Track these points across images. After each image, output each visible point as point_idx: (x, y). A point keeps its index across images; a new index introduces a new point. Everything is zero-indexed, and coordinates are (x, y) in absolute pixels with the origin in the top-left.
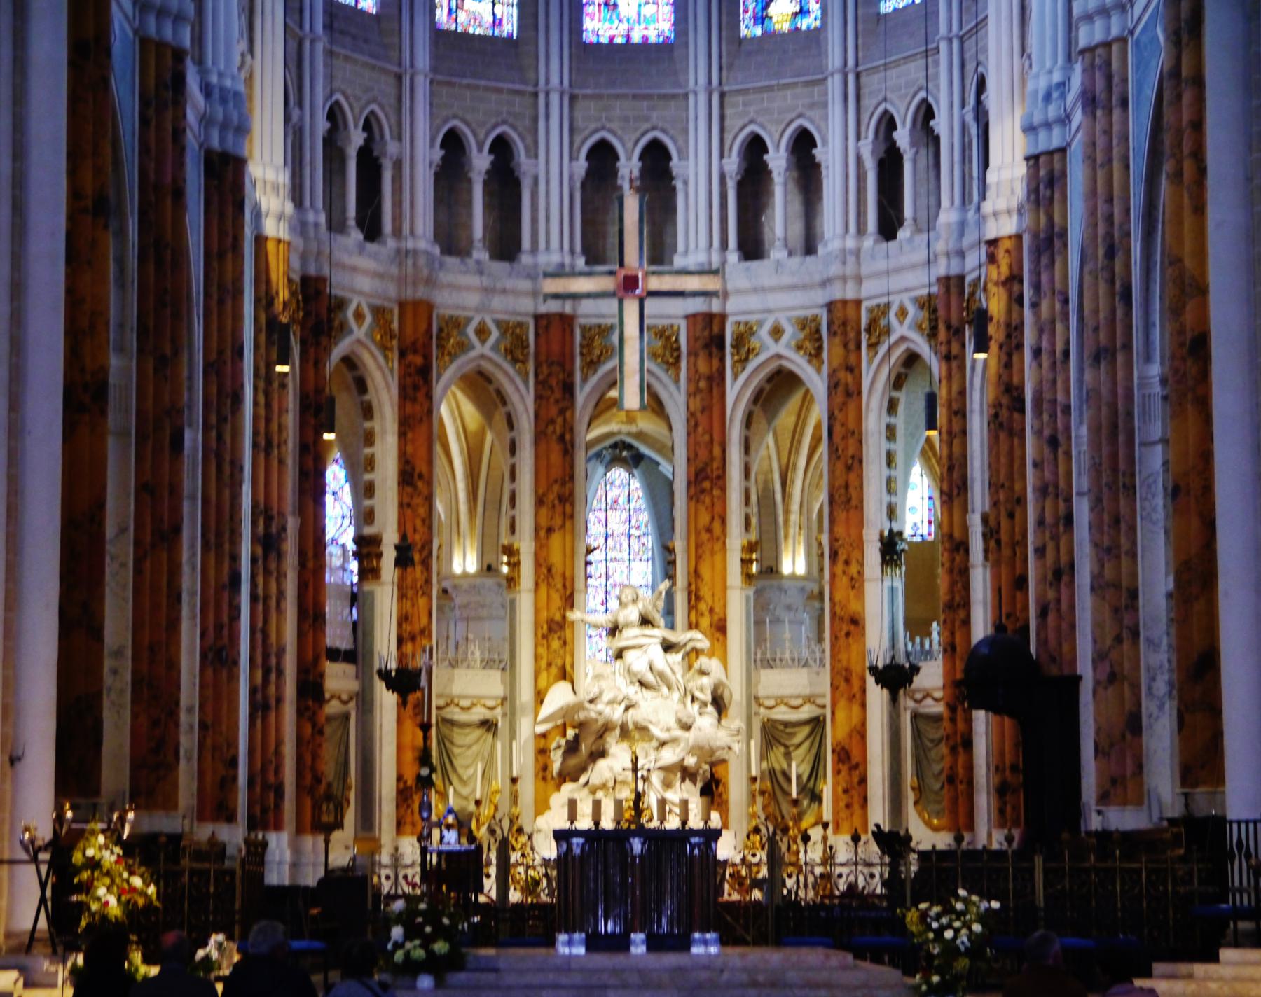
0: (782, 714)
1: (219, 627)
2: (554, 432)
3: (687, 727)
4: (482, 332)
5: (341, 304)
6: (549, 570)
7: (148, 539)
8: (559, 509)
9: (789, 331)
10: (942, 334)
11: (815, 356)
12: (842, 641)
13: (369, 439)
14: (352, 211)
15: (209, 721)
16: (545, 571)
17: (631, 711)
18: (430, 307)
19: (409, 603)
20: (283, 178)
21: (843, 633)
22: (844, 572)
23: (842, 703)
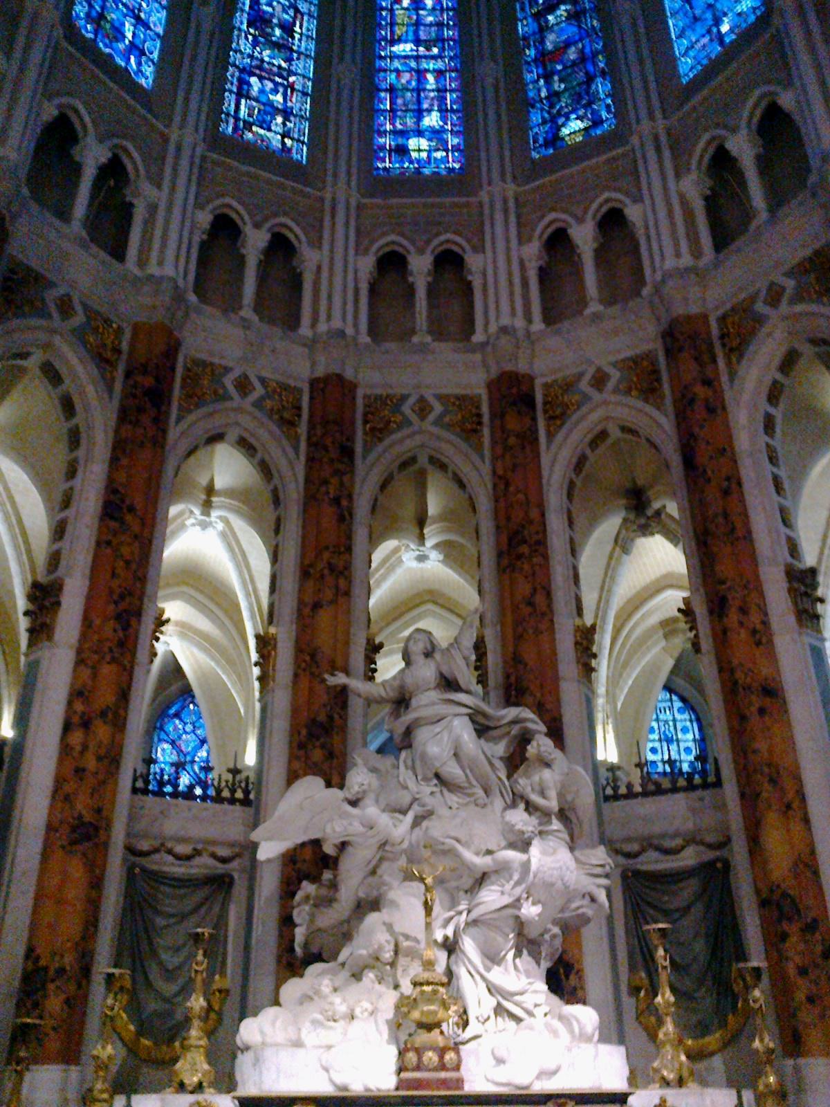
0: (652, 862)
2: (328, 493)
6: (313, 656)
8: (330, 580)
9: (615, 375)
12: (754, 719)
16: (308, 658)
17: (425, 824)
19: (88, 672)
21: (754, 709)
22: (741, 624)
23: (772, 817)
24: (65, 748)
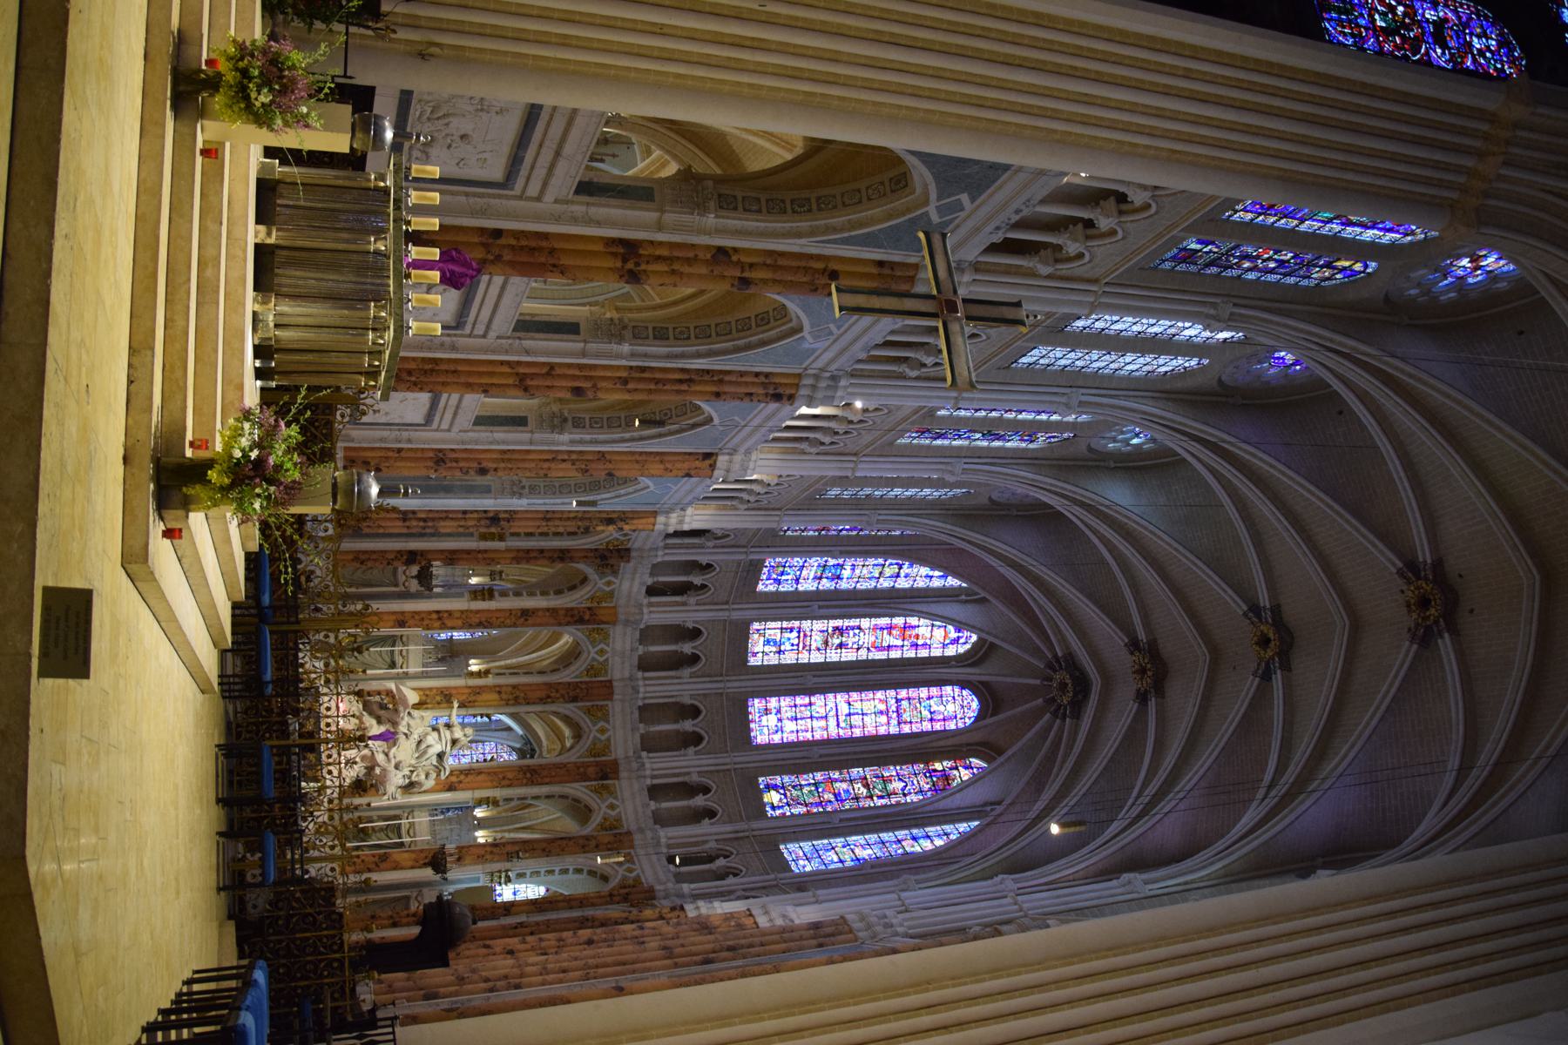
1: (456, 460)
3: (397, 767)
4: (602, 652)
5: (615, 573)
7: (522, 370)
10: (623, 891)
11: (602, 827)
13: (544, 593)
14: (662, 579)
15: (403, 454)
18: (614, 623)
20: (686, 527)
24: (430, 613)
